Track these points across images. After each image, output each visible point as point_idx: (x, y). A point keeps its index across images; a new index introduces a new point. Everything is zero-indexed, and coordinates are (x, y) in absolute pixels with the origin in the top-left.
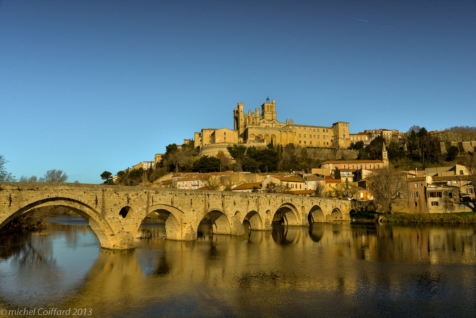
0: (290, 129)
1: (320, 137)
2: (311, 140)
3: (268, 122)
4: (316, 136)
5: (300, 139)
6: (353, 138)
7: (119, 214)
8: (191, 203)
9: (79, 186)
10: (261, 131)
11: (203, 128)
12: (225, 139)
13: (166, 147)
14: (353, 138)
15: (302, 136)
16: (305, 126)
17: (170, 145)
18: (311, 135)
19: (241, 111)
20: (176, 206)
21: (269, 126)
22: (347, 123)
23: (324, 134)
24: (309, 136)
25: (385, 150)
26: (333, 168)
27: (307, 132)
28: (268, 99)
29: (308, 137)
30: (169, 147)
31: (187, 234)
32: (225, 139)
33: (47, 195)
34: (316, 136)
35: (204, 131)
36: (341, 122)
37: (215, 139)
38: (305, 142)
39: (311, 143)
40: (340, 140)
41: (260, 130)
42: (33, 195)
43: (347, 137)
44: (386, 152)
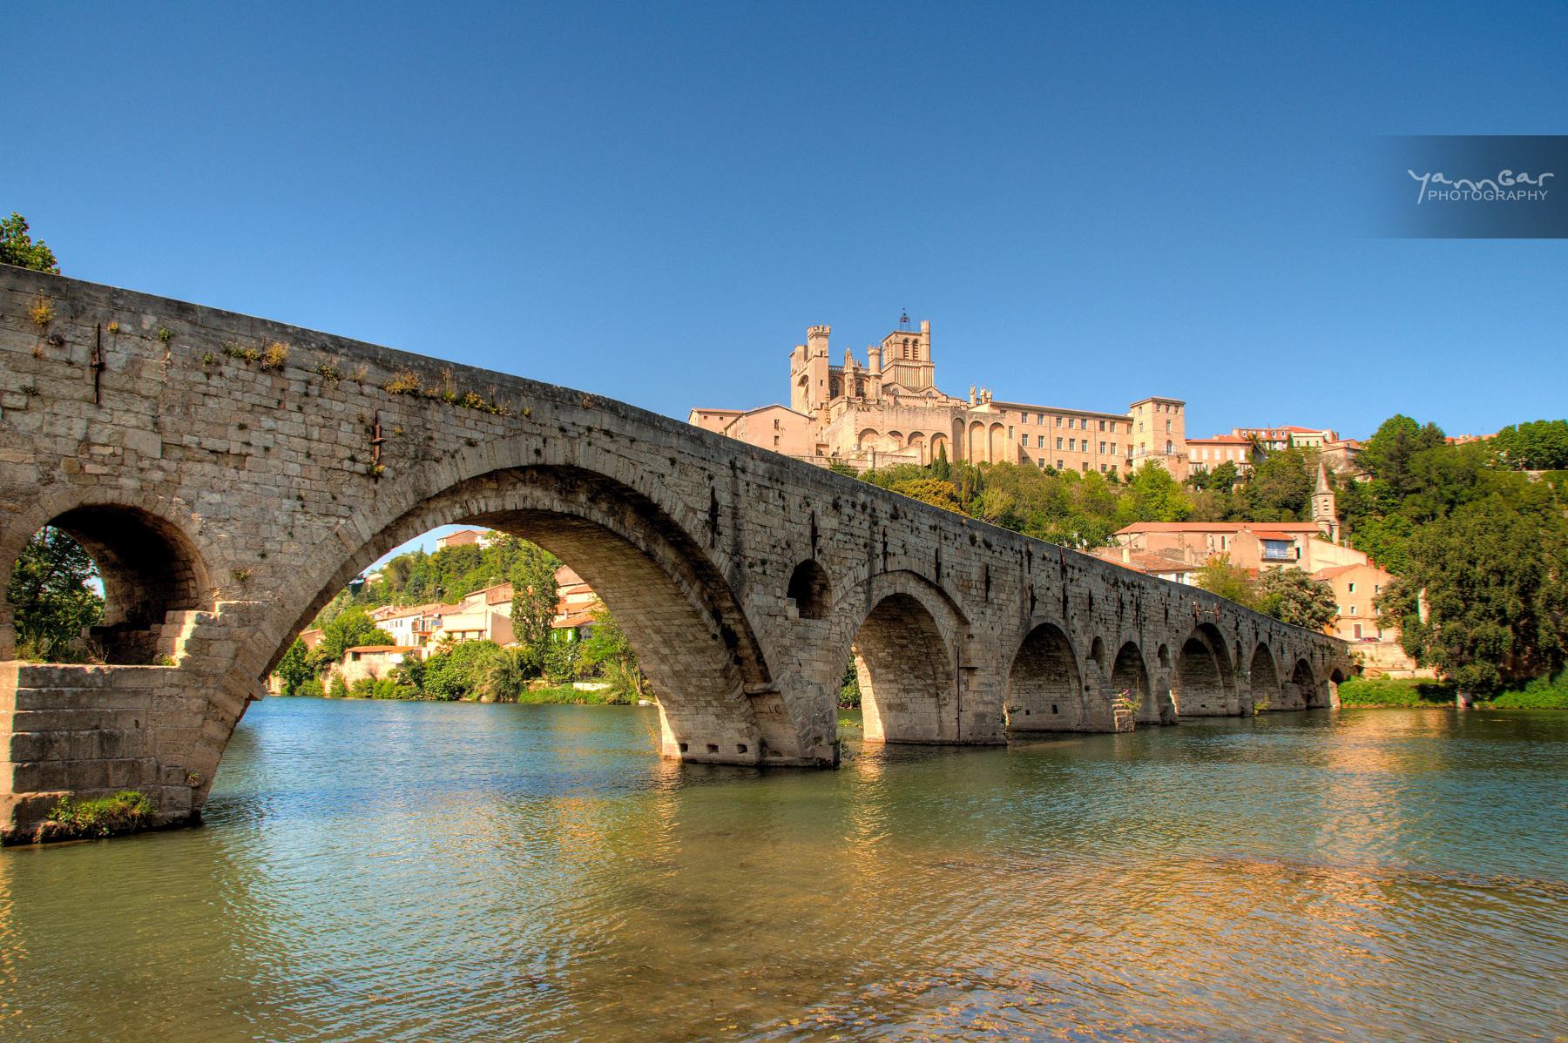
2: (1058, 455)
3: (910, 394)
4: (1077, 445)
6: (1199, 454)
7: (789, 596)
9: (654, 427)
10: (900, 420)
14: (1199, 454)
20: (947, 585)
22: (1178, 405)
23: (1101, 437)
31: (981, 717)
33: (536, 443)
34: (1077, 445)
39: (1060, 463)
42: (476, 436)
44: (1331, 498)
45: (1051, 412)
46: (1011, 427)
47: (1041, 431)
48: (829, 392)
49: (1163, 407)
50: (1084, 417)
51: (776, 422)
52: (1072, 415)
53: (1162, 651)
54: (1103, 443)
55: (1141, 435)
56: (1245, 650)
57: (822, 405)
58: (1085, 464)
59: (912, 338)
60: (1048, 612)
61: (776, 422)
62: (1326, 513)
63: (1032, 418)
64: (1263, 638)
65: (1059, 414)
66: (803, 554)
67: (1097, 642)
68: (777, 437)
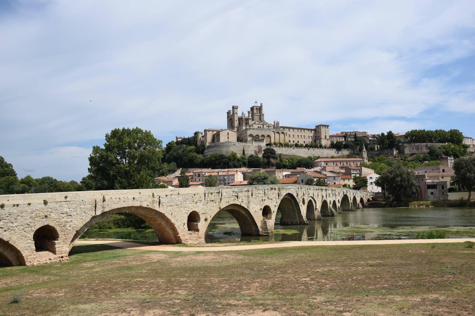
0: (282, 130)
1: (306, 137)
2: (298, 140)
4: (303, 137)
5: (290, 139)
8: (318, 195)
11: (207, 129)
12: (228, 139)
13: (167, 145)
15: (291, 136)
16: (293, 129)
17: (169, 143)
18: (298, 135)
19: (236, 113)
20: (314, 197)
21: (260, 127)
22: (328, 126)
24: (297, 136)
25: (365, 150)
26: (324, 164)
27: (296, 133)
28: (256, 102)
29: (296, 137)
30: (168, 145)
32: (228, 139)
34: (303, 137)
35: (208, 132)
36: (323, 126)
37: (219, 138)
38: (294, 141)
39: (298, 141)
40: (322, 140)
41: (257, 131)
43: (328, 137)
45: (296, 128)
46: (286, 133)
47: (294, 133)
48: (238, 123)
49: (324, 127)
50: (304, 129)
51: (228, 134)
52: (301, 129)
53: (339, 200)
54: (309, 136)
55: (318, 134)
56: (351, 198)
57: (236, 126)
58: (304, 142)
59: (258, 108)
60: (325, 198)
61: (228, 134)
62: (365, 156)
63: (291, 130)
64: (355, 195)
65: (298, 129)
66: (303, 197)
67: (330, 201)
68: (228, 137)
